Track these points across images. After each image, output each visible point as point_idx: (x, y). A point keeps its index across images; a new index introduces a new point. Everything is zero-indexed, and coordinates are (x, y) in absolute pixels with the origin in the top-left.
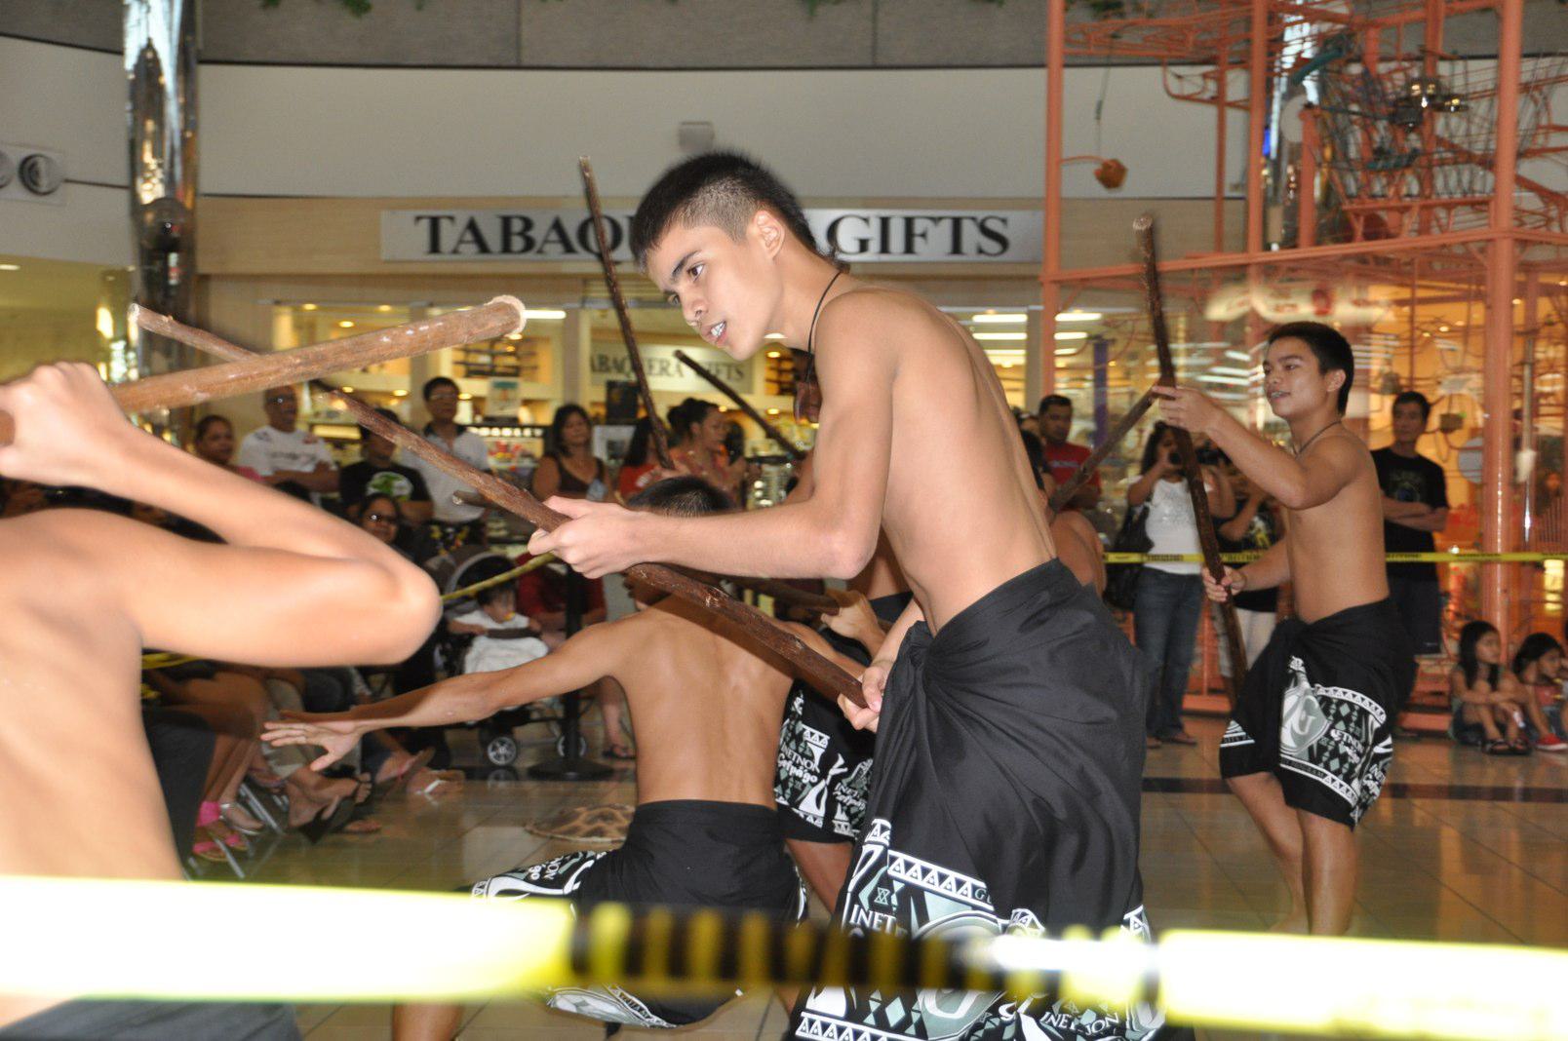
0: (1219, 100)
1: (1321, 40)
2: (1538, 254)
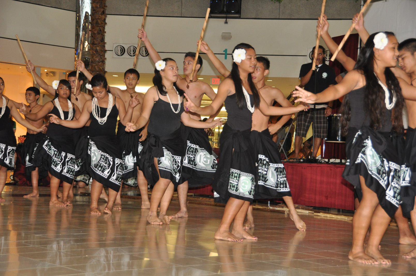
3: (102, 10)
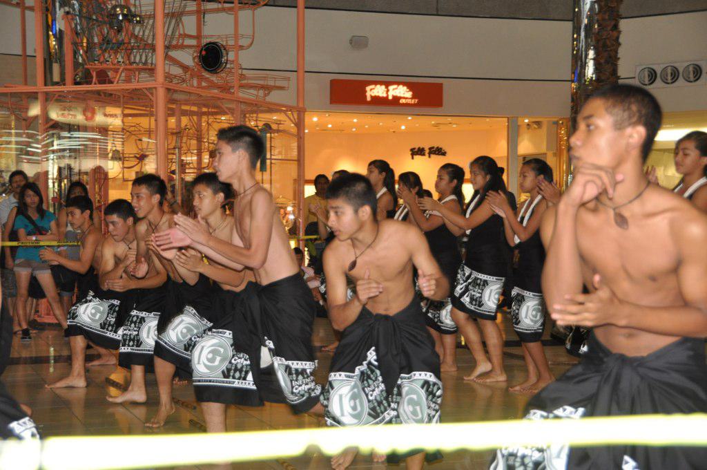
2: (176, 96)
3: (613, 23)
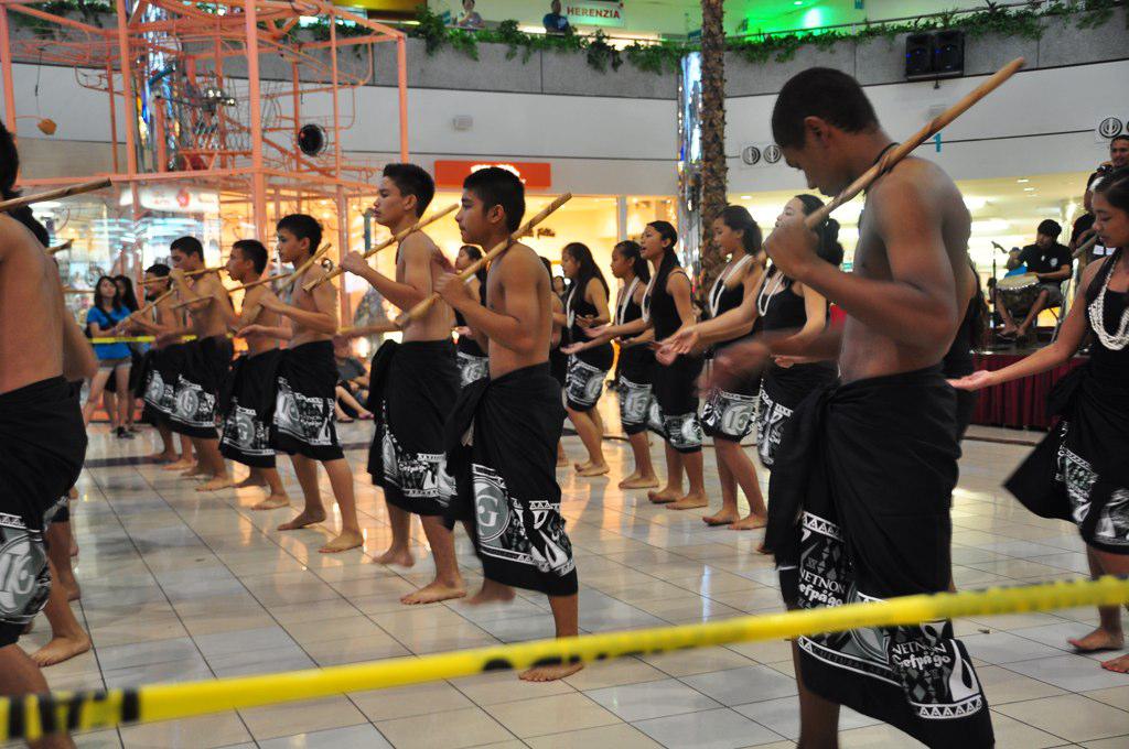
0: (109, 89)
1: (168, 62)
2: (277, 181)
